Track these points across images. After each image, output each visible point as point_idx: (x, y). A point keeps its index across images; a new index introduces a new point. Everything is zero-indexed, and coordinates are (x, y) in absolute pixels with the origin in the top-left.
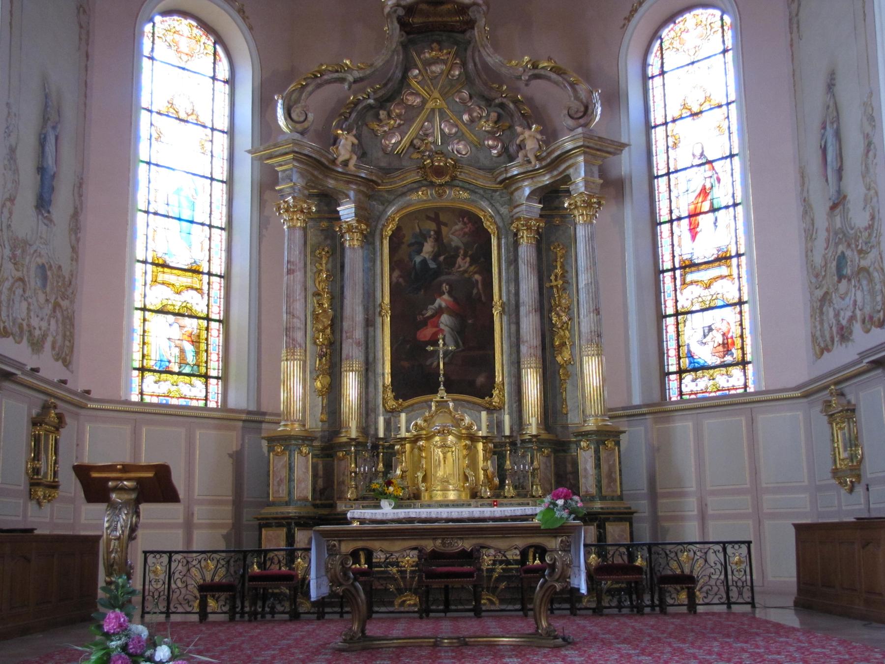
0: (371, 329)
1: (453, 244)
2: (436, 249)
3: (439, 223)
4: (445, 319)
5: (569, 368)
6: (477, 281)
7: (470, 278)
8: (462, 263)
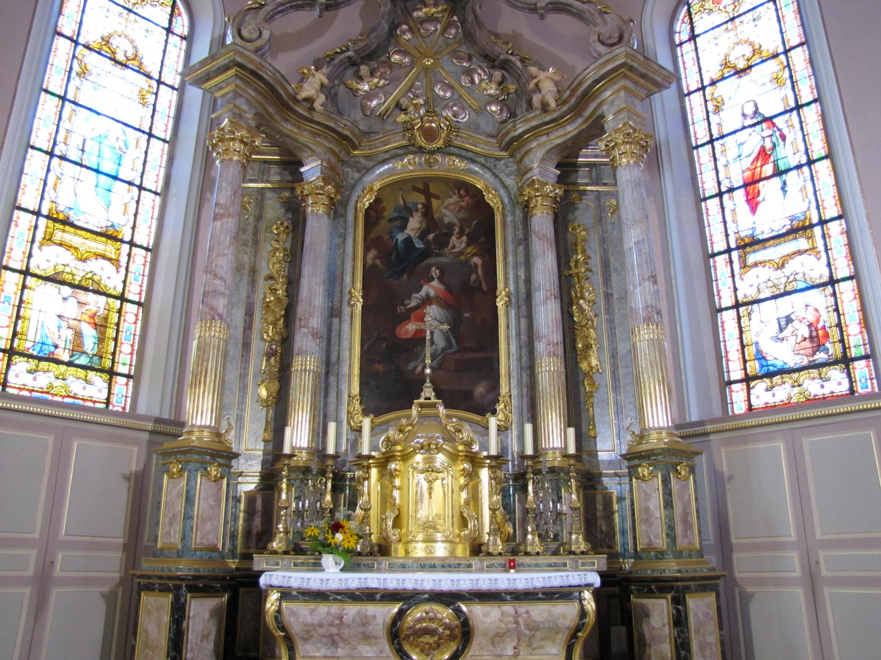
0: (336, 321)
1: (446, 220)
2: (424, 226)
3: (429, 196)
4: (433, 311)
5: (596, 377)
6: (476, 265)
7: (467, 261)
8: (458, 243)
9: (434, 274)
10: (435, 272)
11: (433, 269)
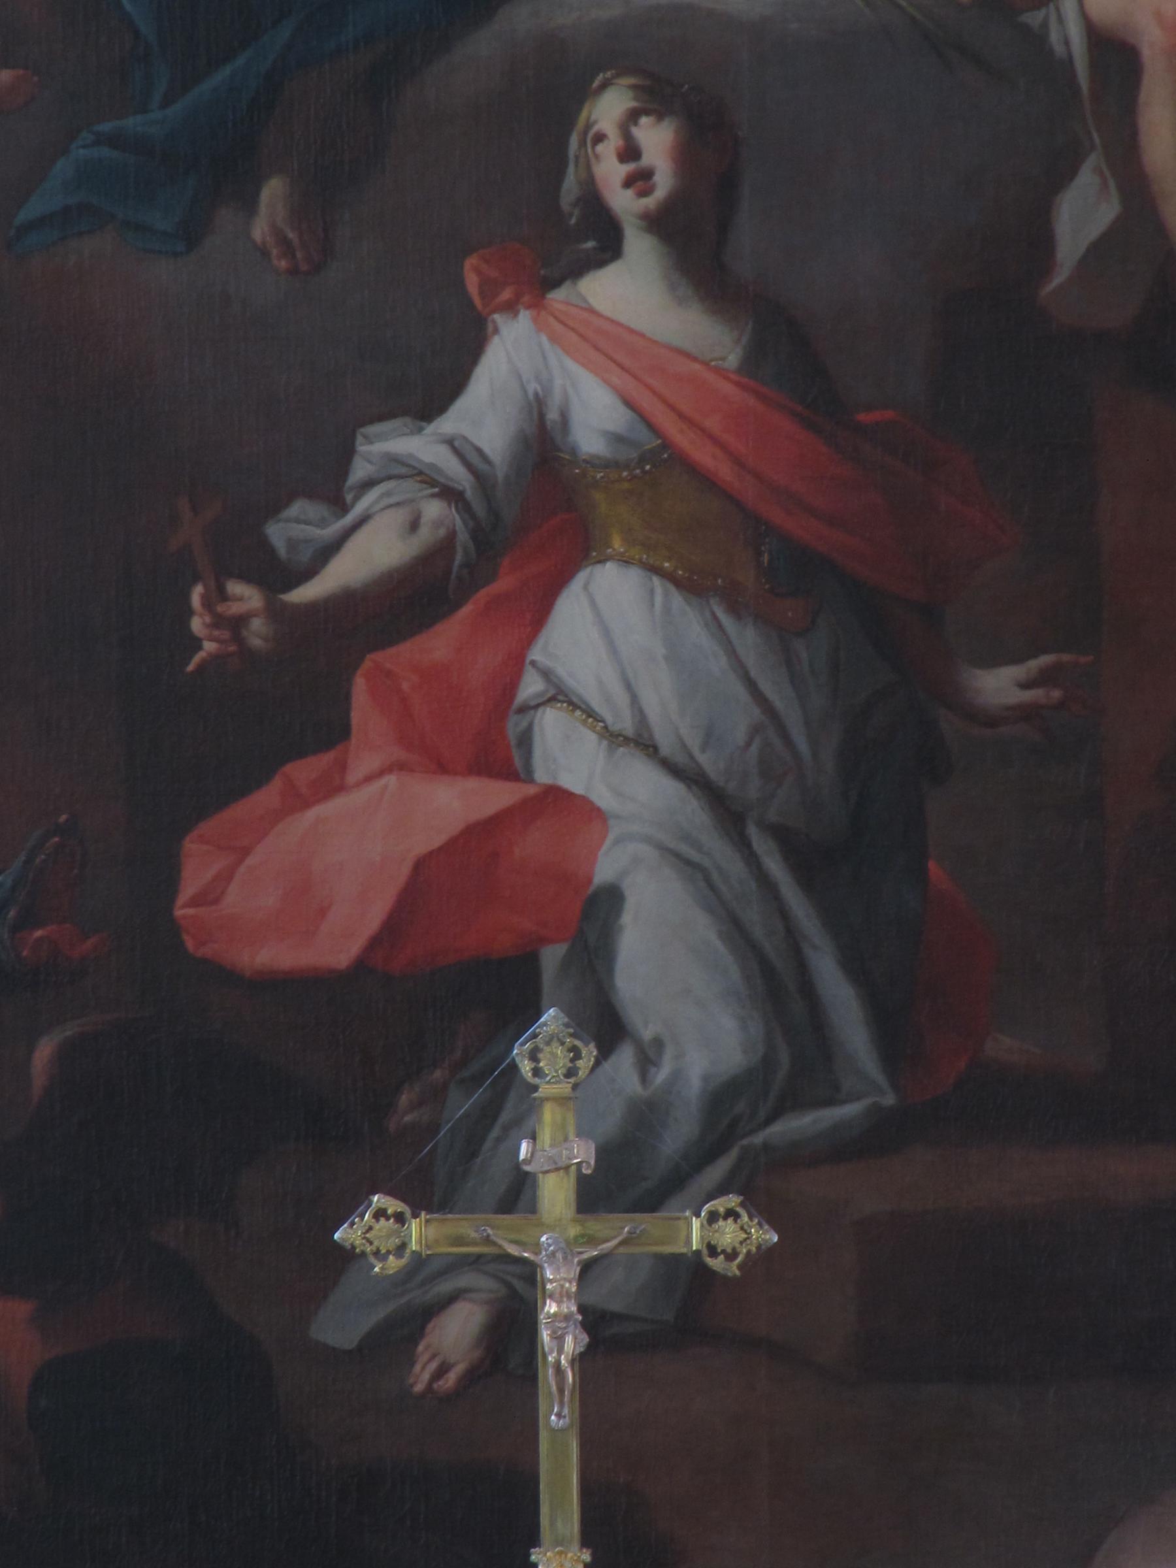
4: (612, 632)
9: (610, 171)
10: (625, 146)
11: (609, 108)
